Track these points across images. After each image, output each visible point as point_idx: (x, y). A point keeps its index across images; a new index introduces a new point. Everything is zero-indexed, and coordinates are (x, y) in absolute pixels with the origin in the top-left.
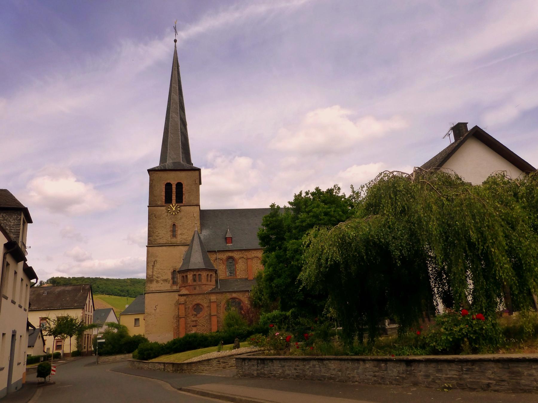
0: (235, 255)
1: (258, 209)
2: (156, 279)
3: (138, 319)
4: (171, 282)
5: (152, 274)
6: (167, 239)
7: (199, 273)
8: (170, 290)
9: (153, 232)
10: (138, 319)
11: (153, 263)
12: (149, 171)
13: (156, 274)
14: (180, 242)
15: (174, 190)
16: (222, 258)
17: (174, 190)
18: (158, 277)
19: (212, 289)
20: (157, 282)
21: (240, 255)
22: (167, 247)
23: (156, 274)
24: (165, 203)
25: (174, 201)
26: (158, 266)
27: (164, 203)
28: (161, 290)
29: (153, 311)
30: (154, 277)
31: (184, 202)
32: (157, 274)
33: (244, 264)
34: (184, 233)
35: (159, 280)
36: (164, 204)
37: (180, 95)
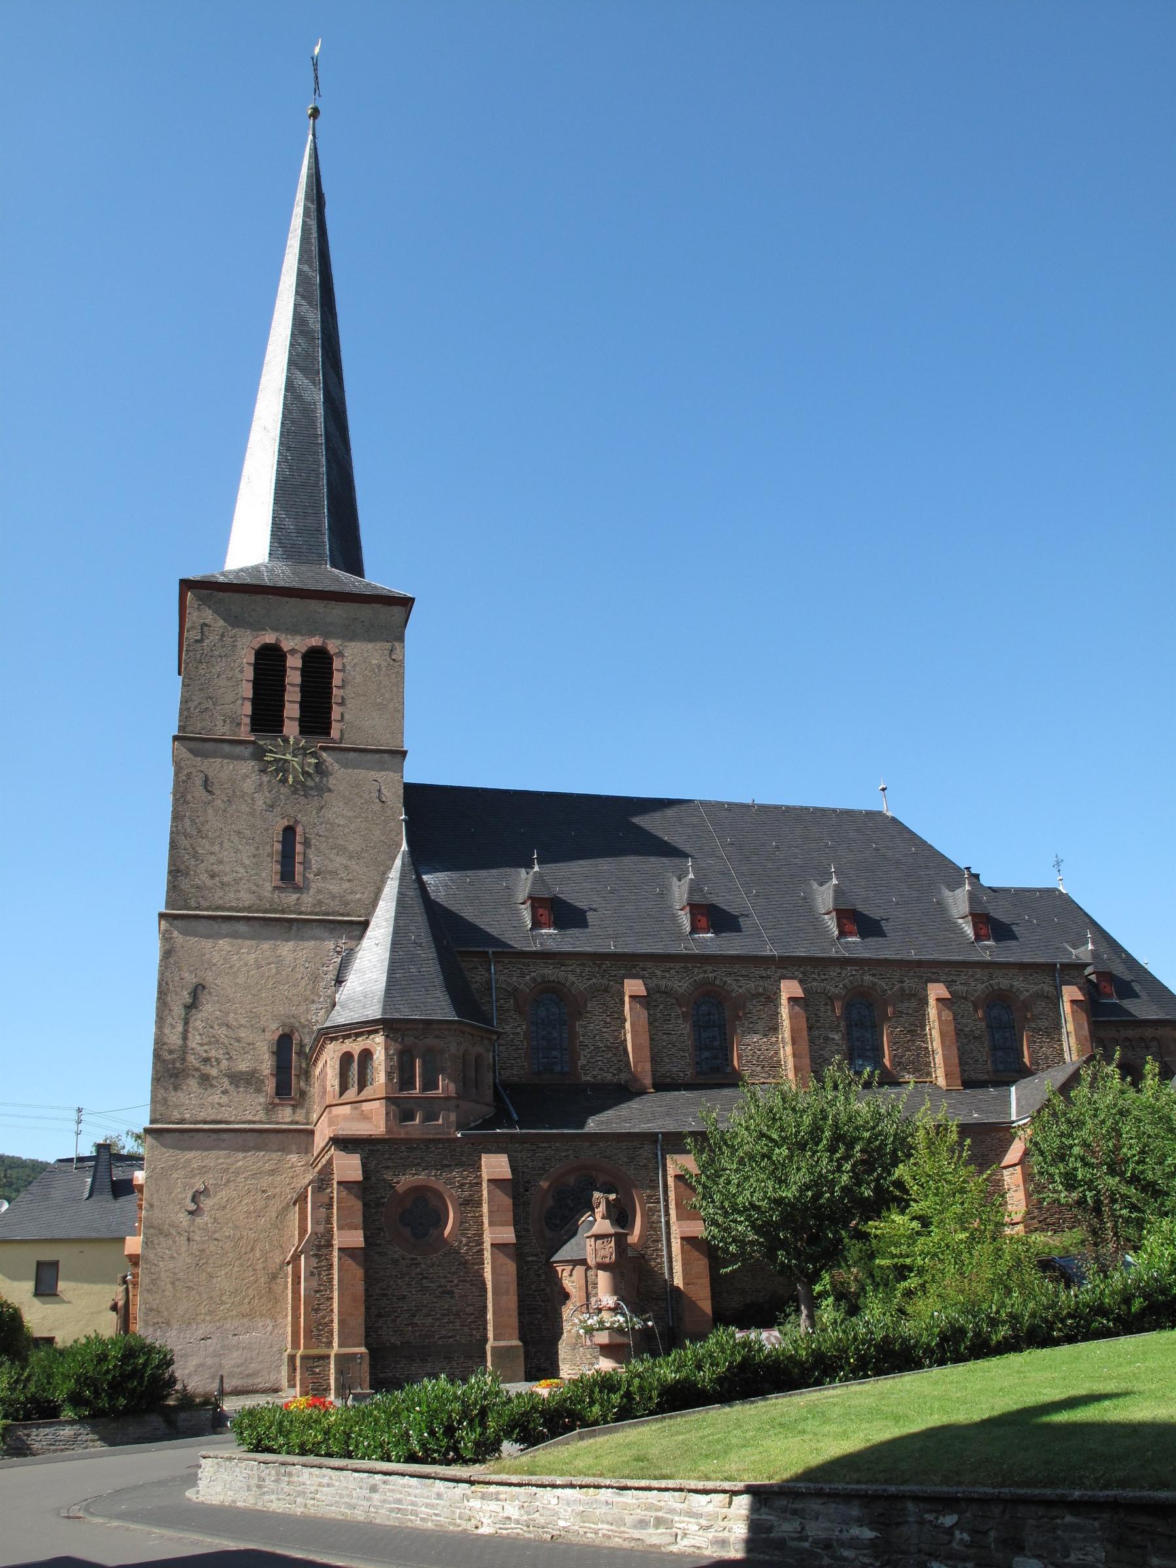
0: (572, 978)
1: (638, 799)
2: (197, 1070)
3: (55, 1264)
4: (270, 1086)
5: (180, 1042)
6: (254, 888)
7: (431, 1041)
8: (254, 1122)
9: (195, 856)
10: (55, 1264)
11: (186, 997)
12: (186, 585)
13: (201, 1045)
14: (314, 905)
15: (293, 677)
16: (516, 989)
17: (293, 677)
18: (206, 1060)
19: (485, 1120)
20: (205, 1080)
21: (594, 980)
22: (256, 924)
23: (201, 1045)
24: (253, 730)
25: (291, 729)
26: (208, 1008)
27: (249, 728)
28: (219, 1118)
29: (183, 1219)
30: (191, 1059)
31: (335, 733)
32: (206, 1047)
33: (608, 1020)
34: (331, 867)
35: (214, 1072)
36: (245, 733)
37: (326, 308)
